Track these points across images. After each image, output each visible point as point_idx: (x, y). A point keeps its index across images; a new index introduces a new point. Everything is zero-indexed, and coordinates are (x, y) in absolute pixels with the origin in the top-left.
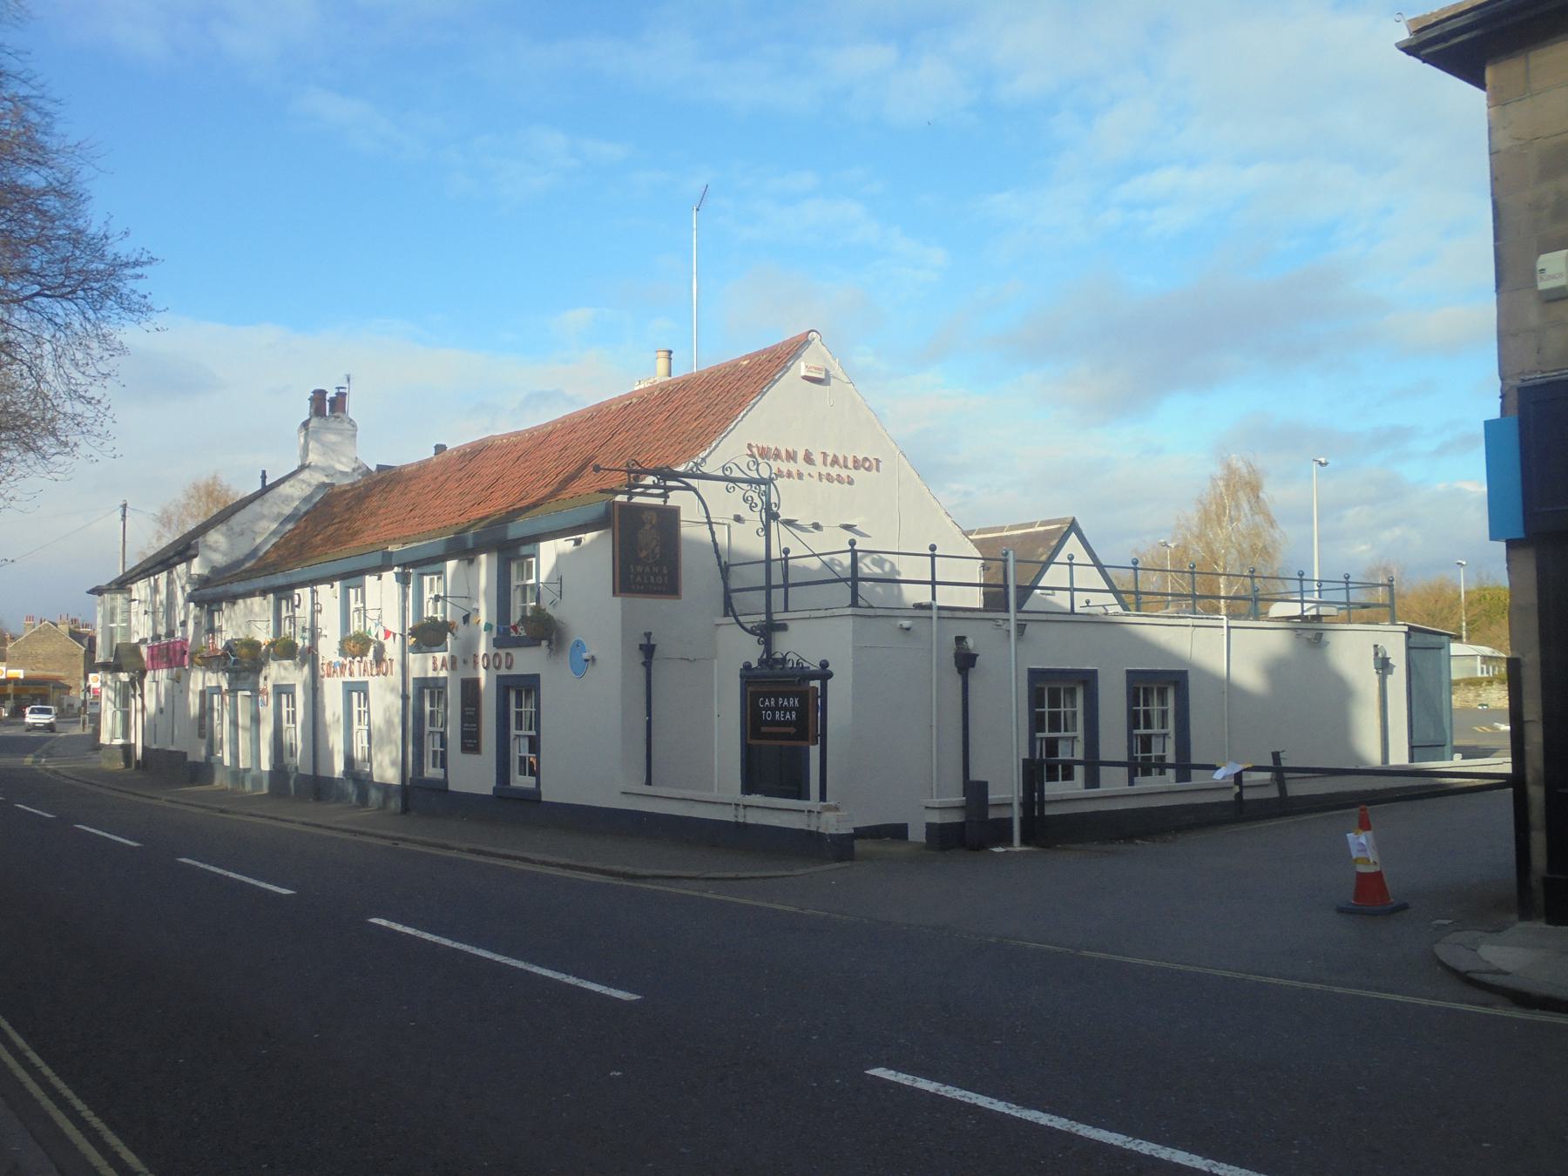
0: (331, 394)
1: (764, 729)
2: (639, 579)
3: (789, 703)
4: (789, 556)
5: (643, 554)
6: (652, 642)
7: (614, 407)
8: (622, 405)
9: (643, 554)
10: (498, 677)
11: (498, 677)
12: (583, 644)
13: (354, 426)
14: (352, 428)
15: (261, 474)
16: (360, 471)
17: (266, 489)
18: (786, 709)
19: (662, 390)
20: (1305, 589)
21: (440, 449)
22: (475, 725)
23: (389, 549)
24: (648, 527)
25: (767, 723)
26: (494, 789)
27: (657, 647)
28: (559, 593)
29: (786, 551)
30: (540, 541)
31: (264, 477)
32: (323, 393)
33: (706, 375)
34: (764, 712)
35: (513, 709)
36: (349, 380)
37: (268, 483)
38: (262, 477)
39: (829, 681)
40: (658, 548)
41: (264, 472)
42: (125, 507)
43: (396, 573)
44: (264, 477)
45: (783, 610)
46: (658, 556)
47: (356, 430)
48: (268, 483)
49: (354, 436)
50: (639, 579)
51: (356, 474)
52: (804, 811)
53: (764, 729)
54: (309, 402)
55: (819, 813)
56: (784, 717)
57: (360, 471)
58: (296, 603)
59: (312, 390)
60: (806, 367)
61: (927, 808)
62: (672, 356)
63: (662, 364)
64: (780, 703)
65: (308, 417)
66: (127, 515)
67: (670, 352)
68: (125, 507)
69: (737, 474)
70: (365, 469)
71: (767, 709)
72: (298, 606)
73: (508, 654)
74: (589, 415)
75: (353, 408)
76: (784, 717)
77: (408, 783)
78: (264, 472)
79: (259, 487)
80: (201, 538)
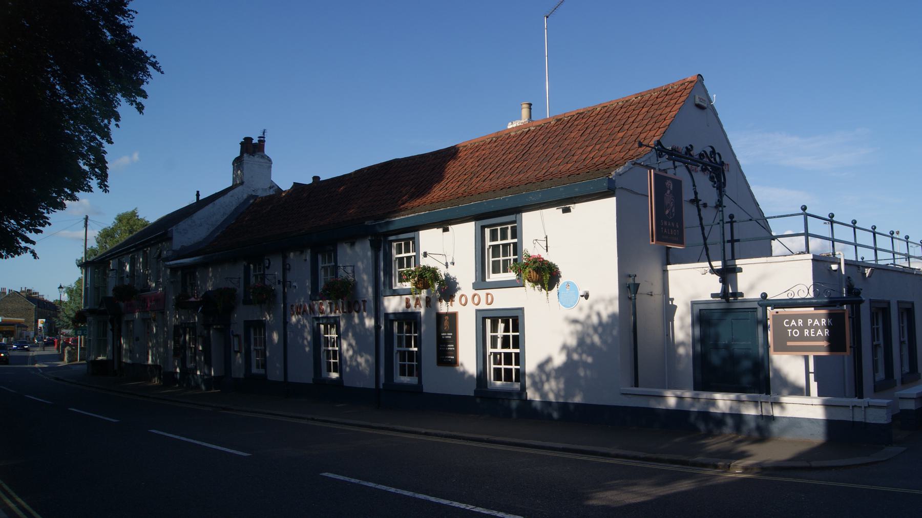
0: (255, 141)
1: (789, 344)
2: (665, 231)
3: (797, 323)
4: (734, 220)
5: (667, 212)
6: (637, 282)
7: (513, 134)
8: (521, 131)
9: (667, 212)
10: (477, 311)
11: (477, 311)
12: (573, 284)
13: (270, 160)
14: (268, 162)
15: (196, 193)
16: (274, 189)
17: (201, 204)
18: (816, 328)
19: (558, 120)
20: (895, 258)
21: (316, 178)
22: (452, 346)
23: (366, 223)
24: (668, 192)
25: (793, 339)
26: (475, 391)
27: (640, 285)
28: (545, 248)
29: (731, 217)
30: (522, 213)
31: (198, 194)
32: (251, 139)
33: (599, 109)
34: (789, 330)
35: (489, 334)
36: (264, 134)
37: (201, 198)
38: (196, 195)
39: (861, 305)
40: (674, 209)
41: (198, 192)
42: (86, 219)
43: (369, 240)
44: (198, 194)
45: (731, 259)
46: (674, 215)
47: (272, 163)
48: (201, 198)
49: (271, 167)
50: (665, 231)
51: (272, 190)
52: (849, 406)
53: (789, 344)
54: (240, 145)
55: (865, 407)
56: (815, 333)
57: (274, 189)
58: (267, 265)
59: (243, 138)
60: (699, 98)
61: (900, 398)
62: (532, 107)
63: (525, 112)
64: (809, 323)
65: (238, 155)
66: (88, 224)
67: (530, 105)
68: (86, 219)
69: (706, 160)
70: (276, 187)
71: (793, 327)
72: (268, 268)
73: (488, 294)
74: (489, 140)
75: (268, 151)
76: (815, 333)
77: (381, 387)
78: (198, 192)
79: (194, 200)
80: (174, 227)
